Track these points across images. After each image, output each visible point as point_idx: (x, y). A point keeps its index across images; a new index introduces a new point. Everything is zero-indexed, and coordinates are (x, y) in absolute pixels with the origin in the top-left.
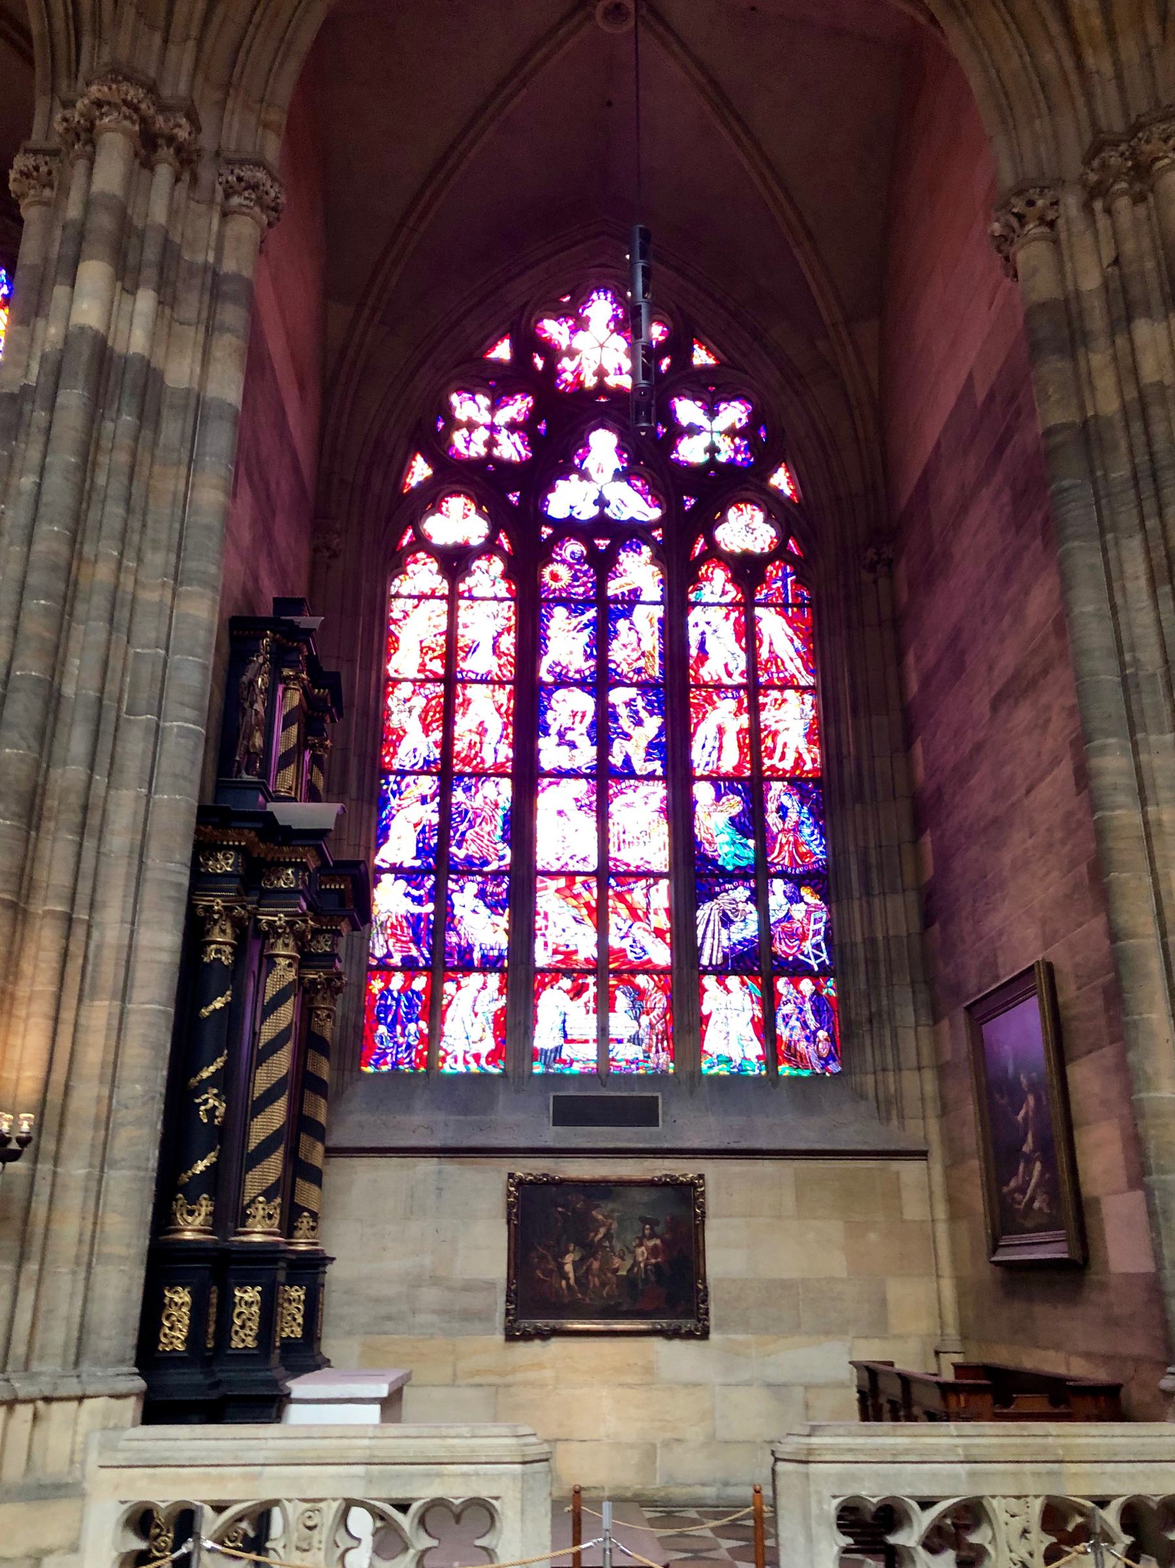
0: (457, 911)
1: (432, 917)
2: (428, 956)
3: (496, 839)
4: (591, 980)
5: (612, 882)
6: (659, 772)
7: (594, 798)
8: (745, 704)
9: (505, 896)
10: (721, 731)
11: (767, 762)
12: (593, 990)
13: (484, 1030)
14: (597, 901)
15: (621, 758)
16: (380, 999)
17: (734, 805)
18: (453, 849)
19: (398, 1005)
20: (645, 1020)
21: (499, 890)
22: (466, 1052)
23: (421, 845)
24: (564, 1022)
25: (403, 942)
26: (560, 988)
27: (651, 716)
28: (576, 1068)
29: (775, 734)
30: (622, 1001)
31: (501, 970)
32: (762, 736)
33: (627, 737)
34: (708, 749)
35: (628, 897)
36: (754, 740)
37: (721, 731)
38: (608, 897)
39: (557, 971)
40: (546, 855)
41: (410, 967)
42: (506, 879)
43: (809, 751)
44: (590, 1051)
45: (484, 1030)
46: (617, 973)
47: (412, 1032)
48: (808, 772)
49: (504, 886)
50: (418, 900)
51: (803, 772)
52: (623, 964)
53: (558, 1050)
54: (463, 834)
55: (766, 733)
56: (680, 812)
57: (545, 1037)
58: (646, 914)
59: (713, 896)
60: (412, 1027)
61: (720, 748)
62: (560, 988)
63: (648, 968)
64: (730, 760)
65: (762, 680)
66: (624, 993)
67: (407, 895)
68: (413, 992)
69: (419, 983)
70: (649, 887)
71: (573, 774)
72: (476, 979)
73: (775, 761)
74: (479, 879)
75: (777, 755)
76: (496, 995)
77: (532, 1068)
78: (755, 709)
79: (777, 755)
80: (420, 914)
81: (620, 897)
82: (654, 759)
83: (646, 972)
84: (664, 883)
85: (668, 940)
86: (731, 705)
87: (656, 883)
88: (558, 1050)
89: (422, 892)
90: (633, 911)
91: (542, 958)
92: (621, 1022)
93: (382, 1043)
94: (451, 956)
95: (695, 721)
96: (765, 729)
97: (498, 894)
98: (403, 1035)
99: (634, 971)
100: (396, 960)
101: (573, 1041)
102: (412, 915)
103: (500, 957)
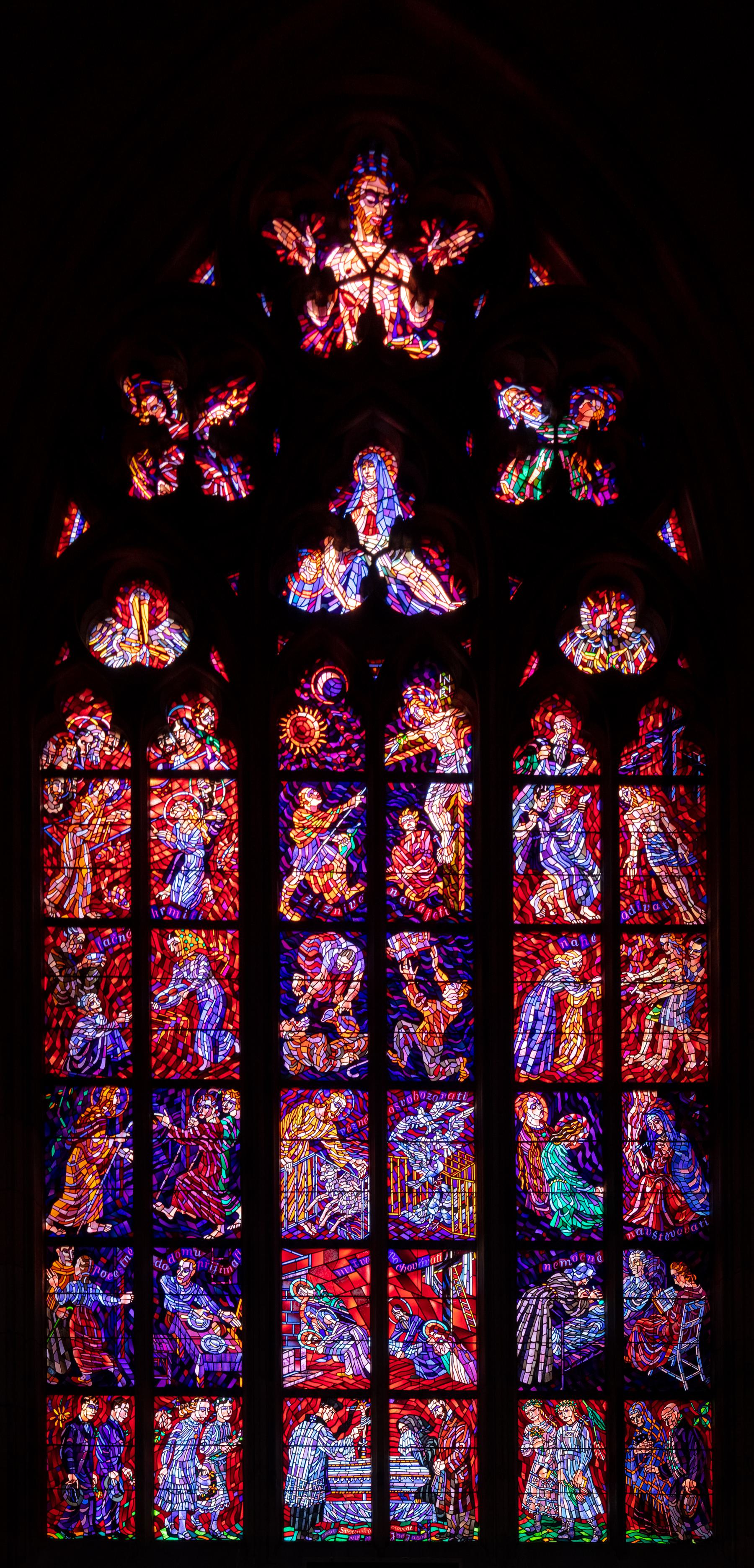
0: (170, 1304)
1: (132, 1312)
2: (129, 1372)
3: (221, 1186)
4: (362, 1408)
5: (393, 1256)
6: (465, 1073)
7: (364, 1121)
8: (597, 961)
9: (236, 1280)
10: (559, 1003)
11: (630, 1060)
12: (365, 1421)
13: (214, 1481)
14: (372, 1286)
15: (407, 1052)
16: (67, 1435)
17: (580, 1130)
18: (159, 1206)
19: (92, 1446)
20: (439, 1466)
21: (228, 1270)
22: (189, 1513)
23: (110, 1199)
24: (326, 1468)
25: (93, 1349)
26: (319, 1420)
27: (451, 981)
28: (342, 1537)
29: (645, 1008)
30: (407, 1440)
31: (233, 1393)
32: (623, 1013)
33: (417, 1017)
34: (538, 1038)
35: (416, 1281)
36: (611, 1018)
37: (559, 1003)
38: (386, 1281)
39: (315, 1393)
40: (294, 1213)
41: (105, 1389)
42: (238, 1253)
43: (694, 1038)
44: (364, 1510)
45: (214, 1481)
46: (401, 1396)
47: (114, 1483)
48: (689, 1074)
49: (235, 1264)
50: (112, 1289)
51: (682, 1074)
52: (410, 1382)
53: (318, 1509)
54: (171, 1182)
55: (628, 1008)
56: (494, 1147)
57: (298, 1491)
58: (445, 1305)
59: (541, 1279)
60: (113, 1475)
61: (559, 1032)
62: (319, 1420)
63: (449, 1391)
64: (574, 1051)
65: (625, 916)
66: (409, 1427)
67: (94, 1279)
68: (111, 1424)
69: (120, 1413)
70: (446, 1264)
71: (334, 1081)
72: (200, 1408)
73: (639, 1057)
74: (198, 1253)
75: (645, 1047)
76: (229, 1429)
77: (282, 1535)
78: (612, 967)
79: (645, 1047)
80: (115, 1307)
81: (404, 1279)
82: (457, 1055)
83: (439, 1395)
84: (468, 1259)
85: (475, 1347)
86: (574, 959)
87: (458, 1258)
88: (318, 1509)
89: (116, 1274)
90: (422, 1297)
91: (292, 1372)
92: (407, 1470)
93: (72, 1499)
94: (163, 1372)
95: (520, 989)
96: (627, 1003)
97: (226, 1278)
98: (101, 1488)
99: (426, 1395)
100: (84, 1377)
101: (339, 1497)
102: (104, 1308)
103: (232, 1374)
